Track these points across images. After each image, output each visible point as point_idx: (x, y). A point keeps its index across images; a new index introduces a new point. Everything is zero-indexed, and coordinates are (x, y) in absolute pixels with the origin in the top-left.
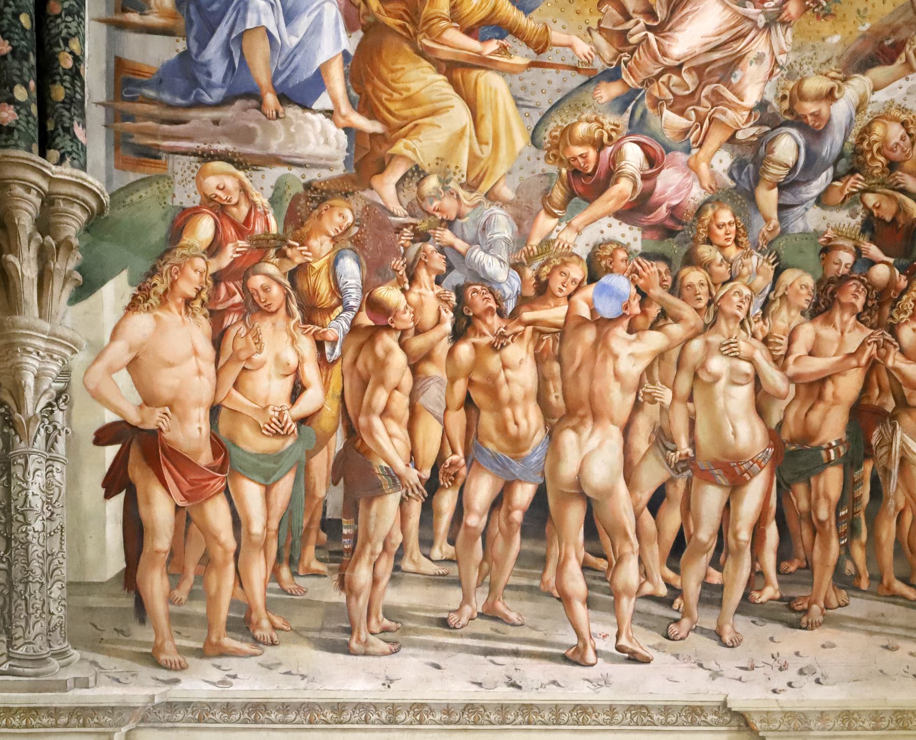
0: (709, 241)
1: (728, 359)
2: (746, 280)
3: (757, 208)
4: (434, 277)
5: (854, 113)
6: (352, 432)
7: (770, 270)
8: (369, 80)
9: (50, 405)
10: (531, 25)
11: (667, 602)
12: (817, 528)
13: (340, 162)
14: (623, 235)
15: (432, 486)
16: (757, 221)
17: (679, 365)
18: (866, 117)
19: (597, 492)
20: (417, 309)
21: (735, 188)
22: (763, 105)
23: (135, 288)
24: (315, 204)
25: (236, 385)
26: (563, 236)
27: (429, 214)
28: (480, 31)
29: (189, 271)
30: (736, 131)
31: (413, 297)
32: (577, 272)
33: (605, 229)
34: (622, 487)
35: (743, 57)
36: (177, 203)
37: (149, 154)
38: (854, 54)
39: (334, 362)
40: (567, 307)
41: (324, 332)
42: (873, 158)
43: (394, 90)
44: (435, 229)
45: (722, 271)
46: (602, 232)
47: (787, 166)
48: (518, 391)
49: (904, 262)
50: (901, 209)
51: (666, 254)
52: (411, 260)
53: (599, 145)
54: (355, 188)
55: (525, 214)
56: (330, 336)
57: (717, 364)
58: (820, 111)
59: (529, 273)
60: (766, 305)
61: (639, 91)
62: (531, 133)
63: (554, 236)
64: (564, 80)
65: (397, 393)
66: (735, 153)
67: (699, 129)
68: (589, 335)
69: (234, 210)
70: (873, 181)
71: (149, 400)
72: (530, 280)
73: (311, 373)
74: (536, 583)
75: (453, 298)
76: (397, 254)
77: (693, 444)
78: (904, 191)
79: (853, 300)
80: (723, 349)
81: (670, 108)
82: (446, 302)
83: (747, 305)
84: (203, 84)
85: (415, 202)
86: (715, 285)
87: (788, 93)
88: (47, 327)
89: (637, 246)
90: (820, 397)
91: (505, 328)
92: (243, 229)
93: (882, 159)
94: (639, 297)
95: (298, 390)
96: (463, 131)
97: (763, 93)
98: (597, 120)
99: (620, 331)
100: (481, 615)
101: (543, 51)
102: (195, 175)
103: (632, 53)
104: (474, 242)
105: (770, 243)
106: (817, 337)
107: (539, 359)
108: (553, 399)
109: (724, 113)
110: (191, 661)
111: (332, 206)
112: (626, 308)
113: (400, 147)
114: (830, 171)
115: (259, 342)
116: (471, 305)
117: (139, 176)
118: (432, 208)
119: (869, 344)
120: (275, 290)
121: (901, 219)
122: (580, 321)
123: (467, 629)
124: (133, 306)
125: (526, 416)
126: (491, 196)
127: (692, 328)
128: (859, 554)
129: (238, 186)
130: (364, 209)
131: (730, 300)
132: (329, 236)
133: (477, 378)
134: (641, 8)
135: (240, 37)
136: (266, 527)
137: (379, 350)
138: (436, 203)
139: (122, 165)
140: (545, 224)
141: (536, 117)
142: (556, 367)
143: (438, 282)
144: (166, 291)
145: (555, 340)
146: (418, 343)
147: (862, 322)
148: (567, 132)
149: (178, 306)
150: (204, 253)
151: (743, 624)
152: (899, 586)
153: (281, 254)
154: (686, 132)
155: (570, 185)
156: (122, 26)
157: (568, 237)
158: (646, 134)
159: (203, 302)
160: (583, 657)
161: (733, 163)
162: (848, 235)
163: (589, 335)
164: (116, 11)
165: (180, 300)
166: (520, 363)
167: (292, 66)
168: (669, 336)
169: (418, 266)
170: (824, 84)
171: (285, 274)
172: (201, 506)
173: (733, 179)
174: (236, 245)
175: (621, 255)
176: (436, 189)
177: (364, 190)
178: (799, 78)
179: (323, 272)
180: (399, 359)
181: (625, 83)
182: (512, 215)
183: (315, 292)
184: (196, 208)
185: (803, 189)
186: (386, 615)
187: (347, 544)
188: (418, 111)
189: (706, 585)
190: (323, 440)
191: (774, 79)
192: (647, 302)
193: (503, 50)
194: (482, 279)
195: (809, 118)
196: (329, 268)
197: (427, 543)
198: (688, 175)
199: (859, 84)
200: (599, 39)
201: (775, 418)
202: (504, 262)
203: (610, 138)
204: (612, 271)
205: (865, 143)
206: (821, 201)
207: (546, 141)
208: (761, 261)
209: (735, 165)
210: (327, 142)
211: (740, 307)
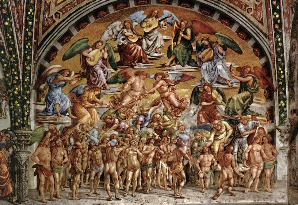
0: (129, 133)
3: (137, 128)
6: (72, 164)
9: (26, 162)
11: (124, 190)
12: (148, 178)
13: (70, 123)
15: (85, 173)
17: (125, 153)
19: (111, 173)
20: (82, 145)
22: (137, 112)
25: (54, 158)
29: (47, 141)
31: (82, 144)
32: (108, 139)
34: (116, 172)
36: (45, 130)
42: (155, 120)
48: (99, 158)
50: (160, 127)
56: (69, 150)
57: (131, 152)
59: (100, 139)
65: (79, 158)
68: (110, 148)
71: (41, 161)
73: (66, 156)
74: (102, 188)
75: (88, 143)
77: (127, 165)
81: (122, 113)
90: (148, 157)
92: (55, 134)
95: (64, 158)
99: (115, 148)
100: (93, 193)
103: (116, 105)
104: (92, 135)
106: (147, 148)
107: (102, 153)
108: (104, 159)
110: (47, 201)
113: (80, 121)
115: (58, 151)
120: (60, 143)
121: (160, 129)
123: (92, 196)
125: (100, 161)
128: (155, 182)
133: (92, 156)
136: (59, 180)
137: (77, 152)
138: (85, 129)
139: (37, 125)
142: (105, 154)
146: (83, 151)
148: (106, 117)
151: (135, 194)
152: (161, 187)
154: (125, 116)
156: (37, 104)
160: (110, 200)
163: (110, 148)
165: (45, 145)
170: (147, 109)
172: (49, 177)
175: (115, 136)
180: (80, 153)
186: (78, 194)
187: (72, 183)
188: (82, 115)
189: (130, 187)
190: (68, 166)
197: (85, 182)
199: (152, 109)
201: (141, 160)
206: (147, 127)
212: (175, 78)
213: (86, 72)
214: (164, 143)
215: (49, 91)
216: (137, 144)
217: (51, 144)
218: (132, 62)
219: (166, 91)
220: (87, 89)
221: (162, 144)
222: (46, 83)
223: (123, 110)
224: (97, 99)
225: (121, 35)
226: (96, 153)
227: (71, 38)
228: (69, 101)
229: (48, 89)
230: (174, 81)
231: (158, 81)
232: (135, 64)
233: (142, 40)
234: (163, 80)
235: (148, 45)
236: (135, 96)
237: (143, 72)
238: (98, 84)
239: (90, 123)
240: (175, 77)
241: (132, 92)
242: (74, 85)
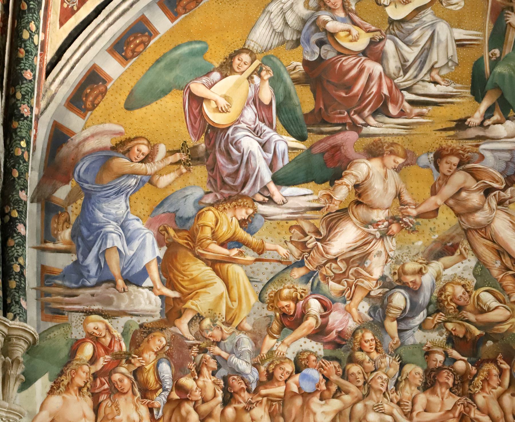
0: (361, 350)
1: (378, 414)
2: (384, 370)
3: (386, 332)
4: (211, 372)
5: (435, 281)
7: (397, 365)
8: (171, 271)
10: (255, 240)
13: (158, 313)
14: (313, 347)
16: (387, 338)
18: (442, 283)
20: (203, 390)
21: (373, 321)
22: (383, 278)
23: (52, 382)
24: (145, 335)
26: (280, 348)
27: (206, 339)
28: (228, 244)
29: (81, 373)
30: (370, 291)
31: (200, 383)
32: (289, 368)
33: (303, 344)
35: (370, 253)
36: (73, 337)
37: (58, 313)
38: (431, 250)
39: (159, 419)
40: (285, 386)
41: (153, 403)
43: (185, 275)
44: (210, 346)
45: (370, 365)
46: (301, 346)
47: (401, 309)
49: (473, 359)
50: (467, 331)
51: (338, 357)
52: (198, 364)
53: (296, 300)
54: (166, 326)
55: (258, 337)
58: (415, 280)
59: (263, 368)
60: (397, 384)
61: (315, 272)
62: (258, 295)
63: (275, 348)
64: (274, 268)
66: (371, 303)
67: (349, 291)
68: (299, 401)
69: (103, 339)
70: (450, 316)
72: (263, 372)
75: (222, 383)
76: (190, 360)
78: (468, 321)
79: (447, 381)
80: (375, 408)
81: (332, 280)
82: (218, 385)
83: (386, 384)
84: (86, 276)
85: (199, 333)
86: (367, 373)
87: (396, 271)
88: (7, 405)
89: (321, 353)
91: (252, 399)
93: (454, 304)
94: (325, 381)
96: (222, 294)
97: (383, 272)
98: (293, 287)
99: (316, 399)
101: (262, 253)
102: (82, 322)
103: (309, 253)
104: (231, 353)
105: (395, 350)
106: (428, 401)
109: (363, 282)
111: (154, 336)
112: (318, 387)
113: (189, 304)
114: (425, 311)
115: (118, 410)
116: (232, 387)
117: (54, 324)
118: (208, 335)
119: (459, 405)
120: (126, 381)
121: (469, 337)
122: (293, 394)
124: (51, 392)
126: (239, 328)
127: (356, 397)
129: (105, 327)
130: (172, 337)
131: (376, 382)
132: (153, 351)
134: (312, 229)
135: (104, 252)
137: (183, 412)
138: (210, 333)
139: (45, 319)
140: (269, 342)
141: (261, 287)
143: (213, 374)
144: (68, 384)
145: (279, 405)
146: (204, 408)
147: (453, 393)
148: (278, 294)
149: (75, 391)
150: (88, 362)
153: (129, 362)
154: (342, 292)
155: (281, 321)
156: (45, 250)
157: (282, 349)
158: (321, 294)
159: (88, 388)
161: (370, 308)
162: (439, 345)
163: (299, 401)
164: (41, 243)
165: (76, 388)
166: (261, 418)
167: (131, 265)
168: (343, 401)
169: (202, 366)
170: (417, 266)
171: (131, 372)
173: (371, 316)
174: (105, 358)
175: (313, 358)
176: (209, 325)
177: (171, 327)
178: (402, 263)
179: (151, 371)
181: (307, 268)
182: (251, 338)
183: (147, 381)
184: (84, 339)
185: (411, 321)
188: (197, 285)
191: (388, 264)
192: (329, 383)
193: (241, 253)
194: (237, 373)
195: (410, 284)
196: (154, 368)
198: (346, 314)
199: (435, 266)
200: (290, 245)
202: (249, 363)
203: (301, 296)
204: (308, 367)
205: (443, 297)
206: (421, 327)
207: (267, 299)
208: (391, 360)
209: (372, 309)
210: (150, 303)
211: (382, 385)
212: (507, 166)
213: (203, 145)
214: (489, 384)
215: (84, 206)
216: (392, 387)
217: (94, 385)
218: (355, 113)
219: (476, 210)
220: (209, 199)
221: (483, 389)
222: (73, 183)
223: (338, 272)
224: (242, 234)
225: (313, 28)
226: (251, 416)
227: (152, 42)
228: (150, 238)
229: (80, 202)
230: (501, 173)
231: (449, 174)
232: (364, 120)
233: (381, 45)
234: (468, 171)
235: (403, 60)
236: (371, 224)
237: (393, 144)
238: (244, 185)
239: (224, 313)
240: (507, 162)
241: (361, 211)
242: (166, 187)
